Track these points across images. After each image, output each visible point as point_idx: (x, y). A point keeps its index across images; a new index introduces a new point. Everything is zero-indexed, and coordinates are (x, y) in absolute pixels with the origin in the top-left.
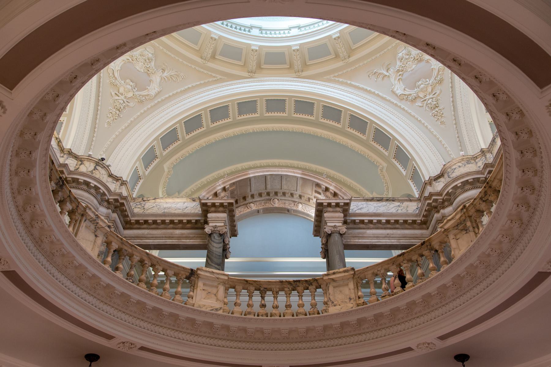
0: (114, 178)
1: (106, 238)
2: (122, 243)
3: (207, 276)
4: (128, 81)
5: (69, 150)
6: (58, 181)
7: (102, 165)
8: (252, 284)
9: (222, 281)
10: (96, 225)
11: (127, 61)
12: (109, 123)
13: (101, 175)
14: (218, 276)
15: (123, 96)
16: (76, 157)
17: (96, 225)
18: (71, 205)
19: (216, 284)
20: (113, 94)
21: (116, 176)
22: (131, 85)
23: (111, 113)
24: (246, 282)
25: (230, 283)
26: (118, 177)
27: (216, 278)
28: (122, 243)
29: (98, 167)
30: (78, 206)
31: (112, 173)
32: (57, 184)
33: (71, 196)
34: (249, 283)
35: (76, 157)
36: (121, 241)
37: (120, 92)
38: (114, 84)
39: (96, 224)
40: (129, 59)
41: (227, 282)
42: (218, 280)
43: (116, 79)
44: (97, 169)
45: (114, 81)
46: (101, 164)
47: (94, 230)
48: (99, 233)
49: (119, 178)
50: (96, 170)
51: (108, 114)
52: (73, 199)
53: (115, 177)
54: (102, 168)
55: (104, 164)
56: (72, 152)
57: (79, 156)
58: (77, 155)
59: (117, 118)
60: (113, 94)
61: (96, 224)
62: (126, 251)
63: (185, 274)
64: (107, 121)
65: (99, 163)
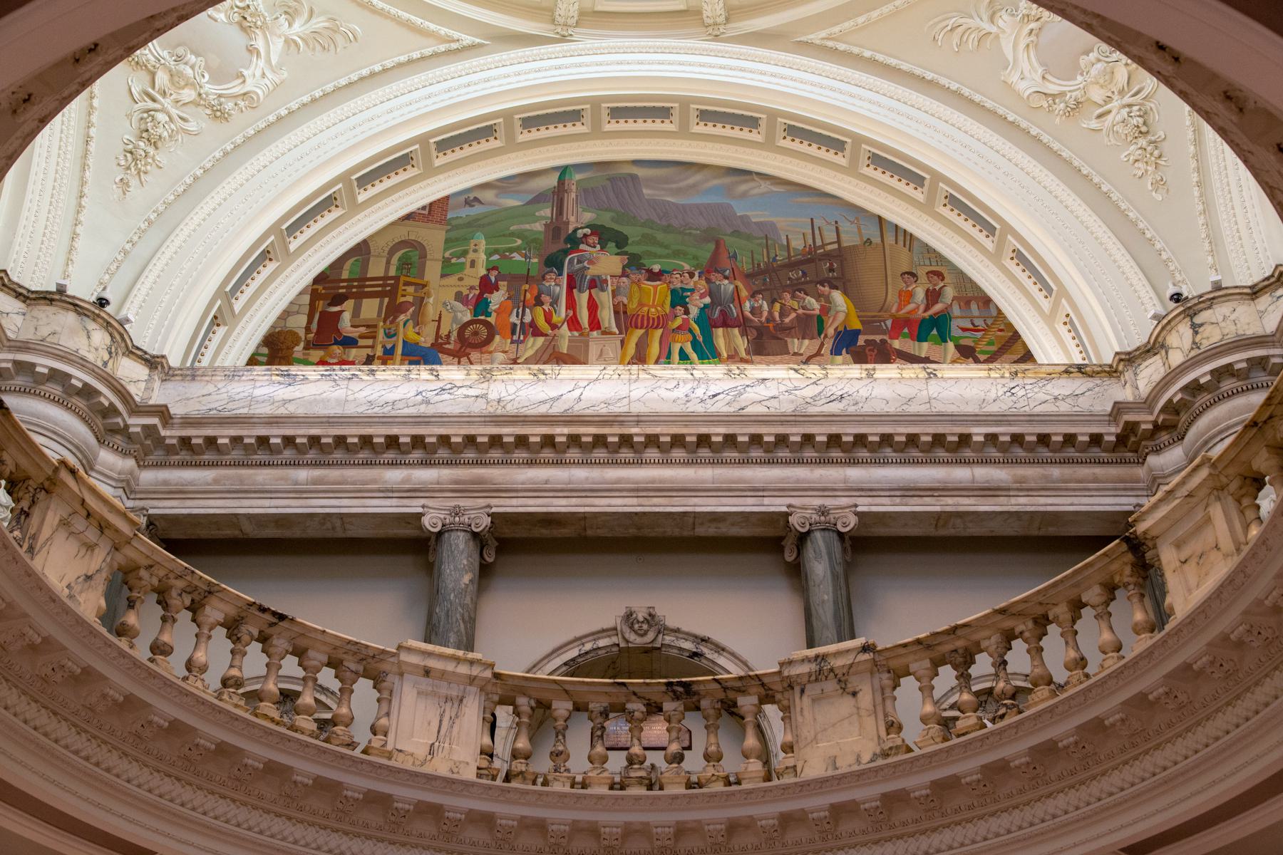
0: (1266, 287)
1: (889, 672)
2: (929, 647)
3: (1165, 518)
4: (1083, 61)
5: (1117, 357)
6: (671, 694)
7: (1200, 303)
8: (1271, 417)
9: (1205, 491)
10: (836, 676)
11: (1033, 38)
12: (1159, 184)
13: (1223, 324)
14: (1184, 491)
15: (1116, 97)
16: (1148, 351)
17: (836, 676)
18: (750, 694)
19: (1199, 515)
20: (1094, 124)
21: (1267, 279)
22: (1094, 61)
23: (1136, 161)
24: (1255, 429)
25: (1231, 471)
26: (1272, 276)
27: (1189, 500)
28: (929, 647)
29: (1197, 320)
30: (763, 685)
31: (1250, 284)
32: (677, 697)
33: (729, 684)
34: (1265, 422)
35: (1148, 351)
36: (921, 647)
37: (1101, 102)
38: (1072, 109)
39: (832, 674)
40: (1032, 30)
41: (1224, 480)
42: (1194, 500)
43: (1062, 94)
44: (1201, 325)
45: (1062, 105)
46: (1195, 305)
47: (838, 687)
48: (854, 682)
49: (1152, 341)
50: (1201, 330)
51: (1136, 172)
52: (739, 684)
53: (1266, 283)
54: (1209, 308)
55: (1201, 296)
56: (1129, 353)
57: (1149, 342)
58: (1145, 345)
59: (1156, 153)
60: (1094, 124)
61: (832, 674)
62: (955, 651)
63: (1126, 564)
64: (1150, 188)
65: (1190, 308)
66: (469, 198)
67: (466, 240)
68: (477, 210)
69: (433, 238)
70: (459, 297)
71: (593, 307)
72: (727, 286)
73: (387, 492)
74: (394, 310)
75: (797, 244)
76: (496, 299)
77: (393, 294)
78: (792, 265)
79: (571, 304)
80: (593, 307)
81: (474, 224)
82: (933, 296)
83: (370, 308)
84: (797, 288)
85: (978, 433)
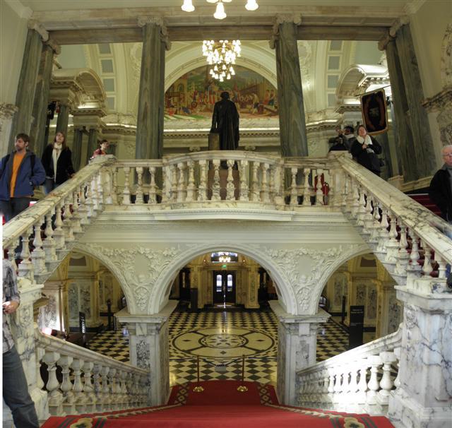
66: (190, 73)
67: (190, 83)
68: (192, 76)
69: (185, 83)
70: (191, 96)
71: (214, 98)
72: (237, 93)
73: (184, 143)
74: (180, 99)
75: (249, 83)
76: (197, 96)
77: (179, 96)
78: (247, 89)
79: (210, 98)
80: (214, 98)
81: (192, 79)
82: (272, 95)
83: (176, 99)
84: (249, 94)
85: (274, 133)
